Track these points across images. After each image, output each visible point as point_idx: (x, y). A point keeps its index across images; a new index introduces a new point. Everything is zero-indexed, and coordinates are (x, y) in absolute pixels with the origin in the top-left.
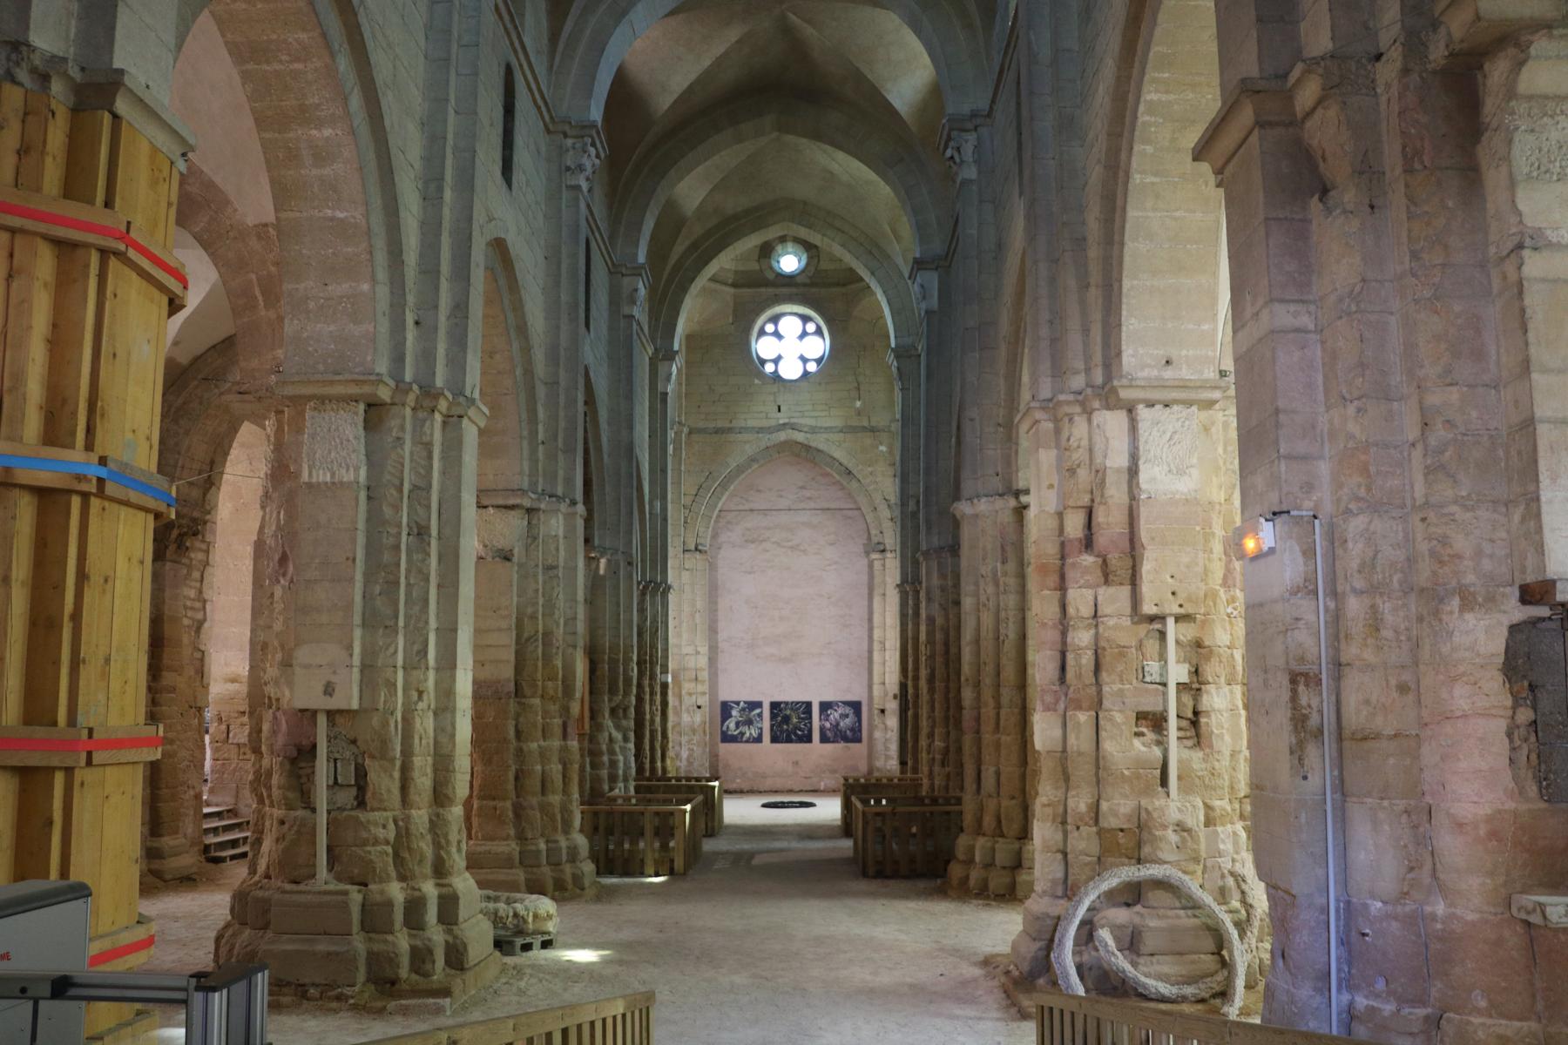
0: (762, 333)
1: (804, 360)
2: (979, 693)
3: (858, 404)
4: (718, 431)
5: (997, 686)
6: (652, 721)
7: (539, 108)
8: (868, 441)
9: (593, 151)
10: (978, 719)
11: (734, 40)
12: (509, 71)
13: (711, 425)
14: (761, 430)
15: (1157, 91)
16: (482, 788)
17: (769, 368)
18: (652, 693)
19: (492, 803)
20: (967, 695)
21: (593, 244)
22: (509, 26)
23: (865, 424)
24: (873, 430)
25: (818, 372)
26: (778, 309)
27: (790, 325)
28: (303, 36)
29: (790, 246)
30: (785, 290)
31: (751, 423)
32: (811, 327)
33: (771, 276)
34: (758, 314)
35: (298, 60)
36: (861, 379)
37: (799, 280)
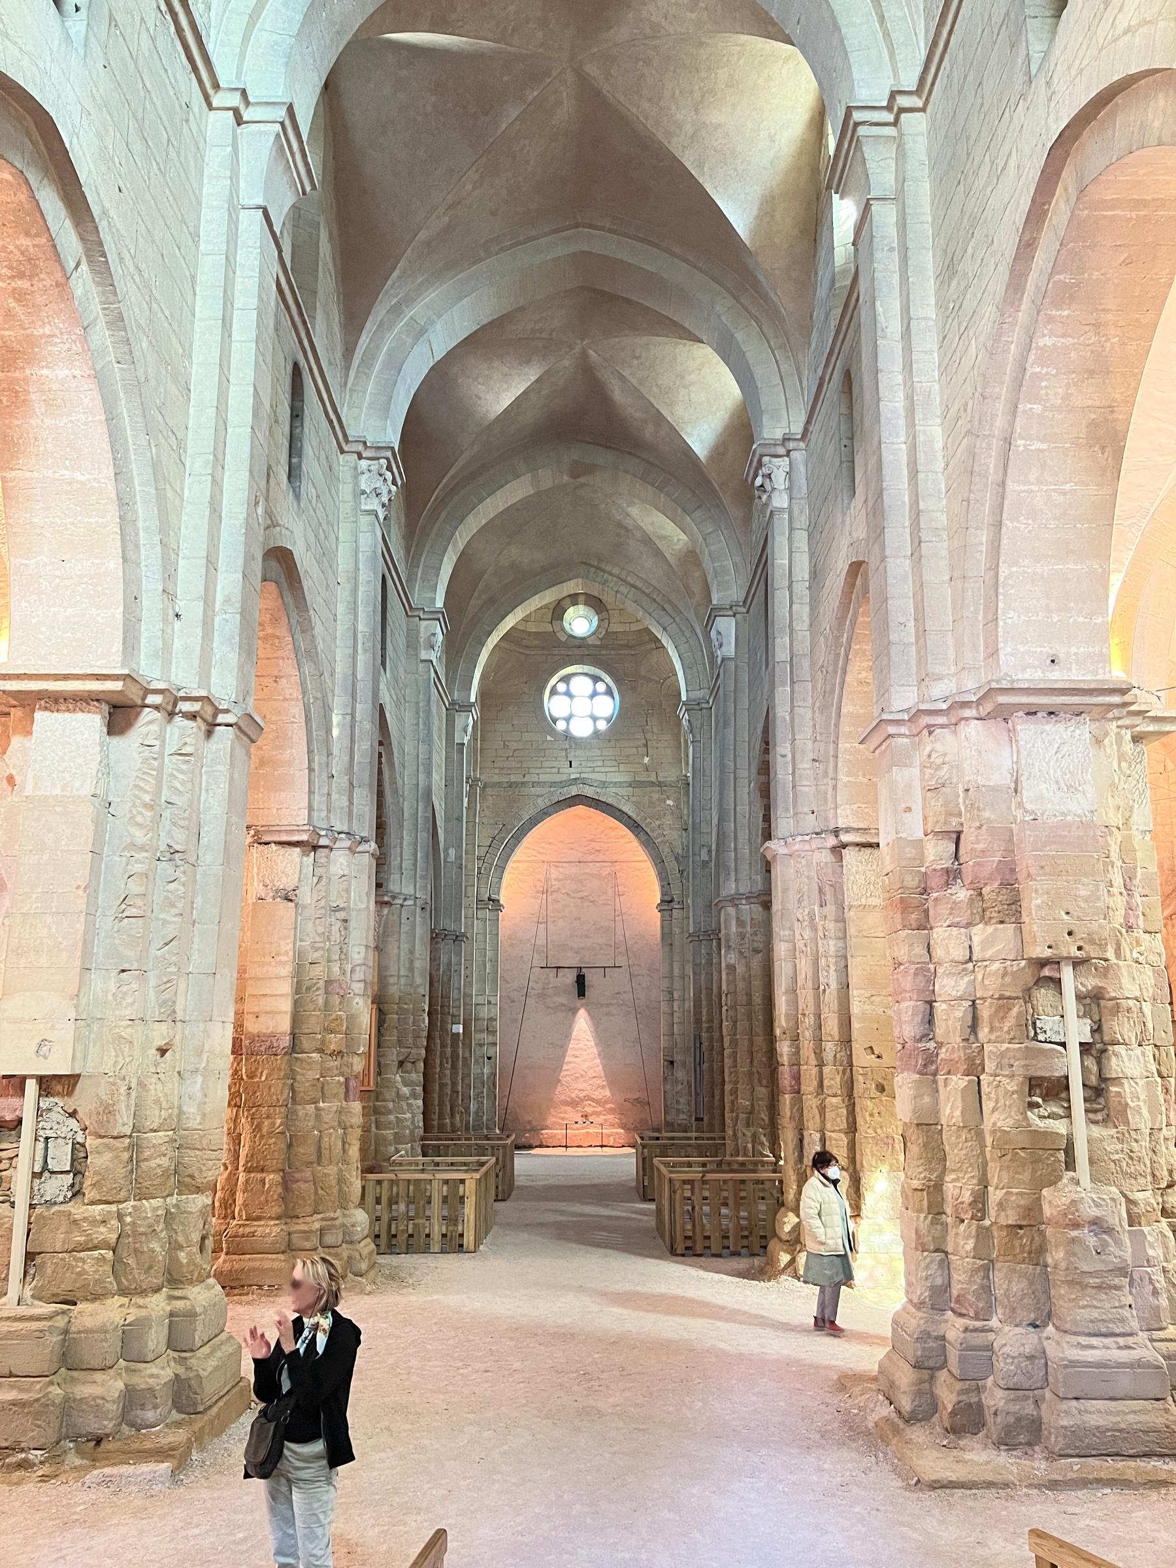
0: (554, 692)
2: (798, 1048)
3: (646, 760)
4: (511, 785)
5: (819, 1040)
6: (442, 1075)
7: (331, 422)
8: (656, 796)
9: (389, 475)
10: (797, 1078)
11: (533, 379)
12: (296, 371)
14: (553, 784)
15: (1052, 334)
16: (251, 1157)
17: (561, 726)
18: (443, 1046)
19: (259, 1176)
20: (784, 1049)
21: (389, 582)
22: (297, 318)
23: (653, 779)
24: (660, 784)
25: (609, 730)
27: (581, 685)
28: (26, 242)
30: (577, 651)
31: (543, 778)
34: (552, 675)
35: (21, 275)
36: (648, 736)
37: (590, 641)
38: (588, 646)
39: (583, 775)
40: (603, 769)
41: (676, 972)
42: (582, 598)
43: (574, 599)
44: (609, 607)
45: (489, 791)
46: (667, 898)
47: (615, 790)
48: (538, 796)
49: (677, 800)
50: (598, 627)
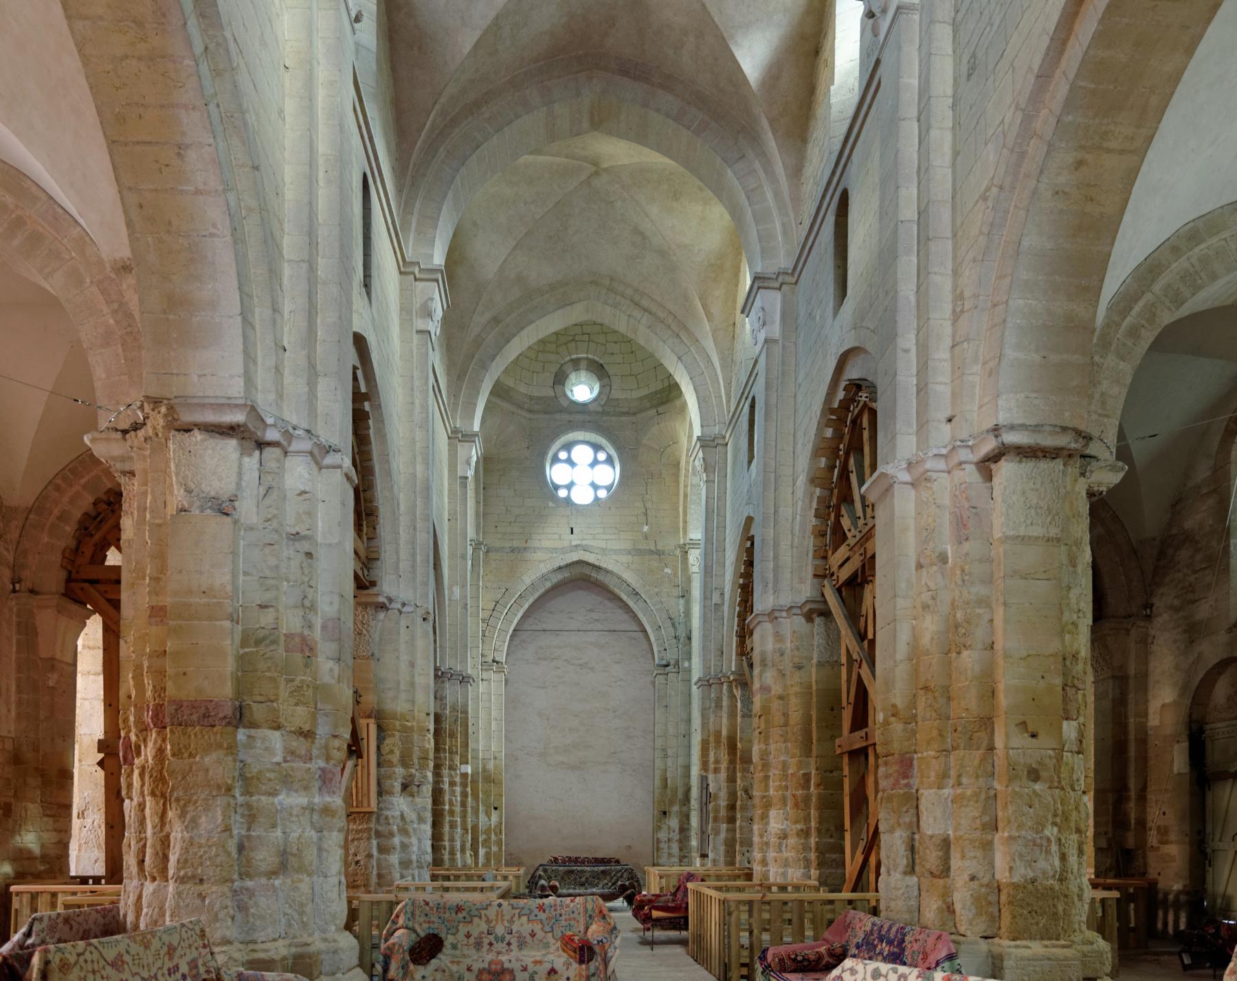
0: (556, 459)
1: (595, 487)
3: (646, 528)
8: (655, 564)
13: (508, 545)
17: (562, 493)
23: (653, 548)
25: (610, 498)
26: (571, 436)
27: (582, 453)
29: (583, 375)
30: (579, 417)
31: (546, 544)
32: (602, 456)
33: (565, 404)
36: (649, 505)
37: (592, 408)
38: (589, 413)
39: (585, 542)
40: (604, 537)
41: (671, 731)
42: (584, 364)
43: (576, 364)
44: (611, 373)
45: (492, 555)
46: (664, 662)
47: (615, 557)
48: (540, 562)
49: (675, 569)
50: (600, 393)
